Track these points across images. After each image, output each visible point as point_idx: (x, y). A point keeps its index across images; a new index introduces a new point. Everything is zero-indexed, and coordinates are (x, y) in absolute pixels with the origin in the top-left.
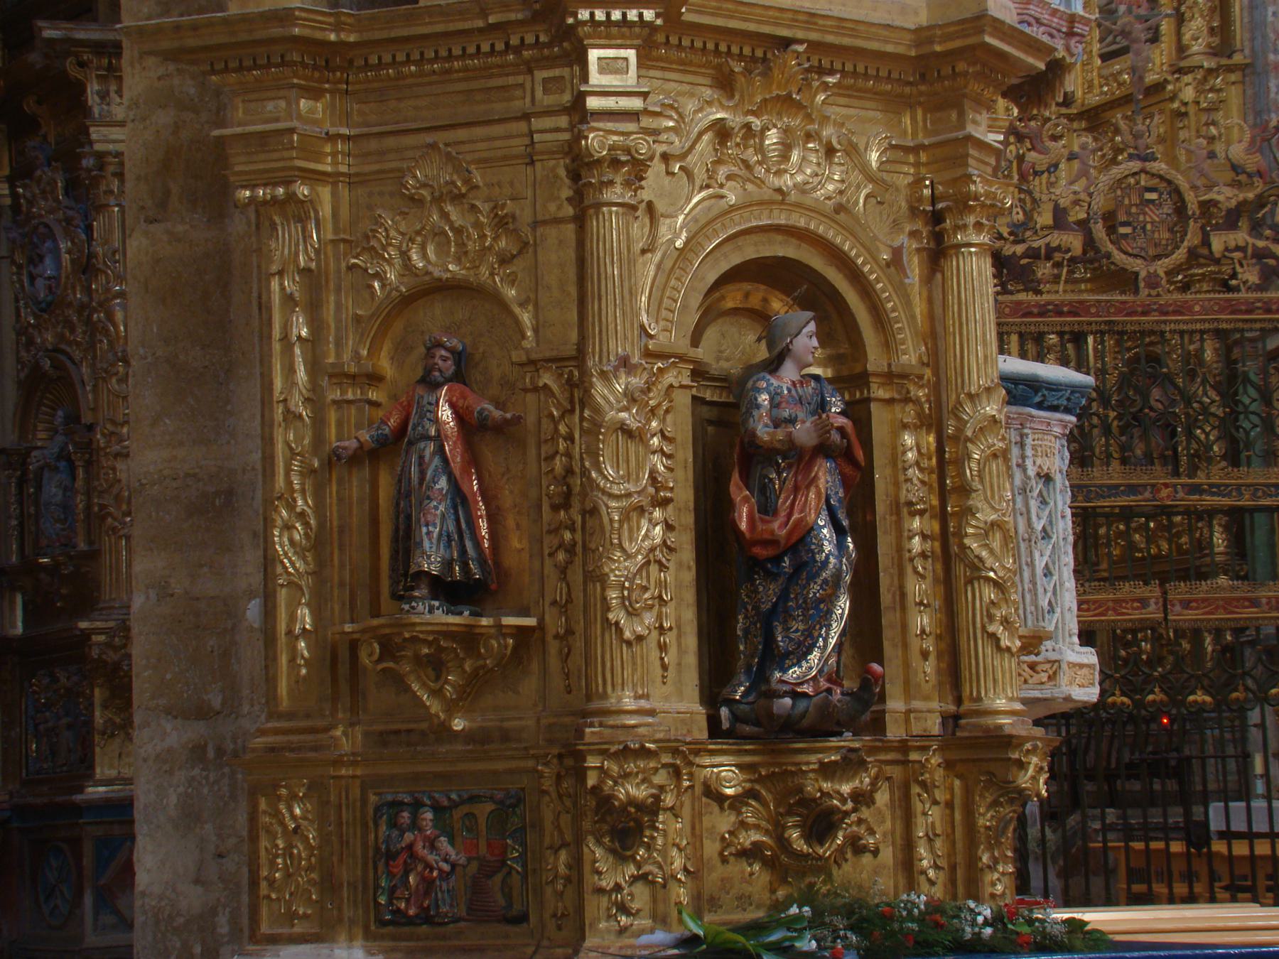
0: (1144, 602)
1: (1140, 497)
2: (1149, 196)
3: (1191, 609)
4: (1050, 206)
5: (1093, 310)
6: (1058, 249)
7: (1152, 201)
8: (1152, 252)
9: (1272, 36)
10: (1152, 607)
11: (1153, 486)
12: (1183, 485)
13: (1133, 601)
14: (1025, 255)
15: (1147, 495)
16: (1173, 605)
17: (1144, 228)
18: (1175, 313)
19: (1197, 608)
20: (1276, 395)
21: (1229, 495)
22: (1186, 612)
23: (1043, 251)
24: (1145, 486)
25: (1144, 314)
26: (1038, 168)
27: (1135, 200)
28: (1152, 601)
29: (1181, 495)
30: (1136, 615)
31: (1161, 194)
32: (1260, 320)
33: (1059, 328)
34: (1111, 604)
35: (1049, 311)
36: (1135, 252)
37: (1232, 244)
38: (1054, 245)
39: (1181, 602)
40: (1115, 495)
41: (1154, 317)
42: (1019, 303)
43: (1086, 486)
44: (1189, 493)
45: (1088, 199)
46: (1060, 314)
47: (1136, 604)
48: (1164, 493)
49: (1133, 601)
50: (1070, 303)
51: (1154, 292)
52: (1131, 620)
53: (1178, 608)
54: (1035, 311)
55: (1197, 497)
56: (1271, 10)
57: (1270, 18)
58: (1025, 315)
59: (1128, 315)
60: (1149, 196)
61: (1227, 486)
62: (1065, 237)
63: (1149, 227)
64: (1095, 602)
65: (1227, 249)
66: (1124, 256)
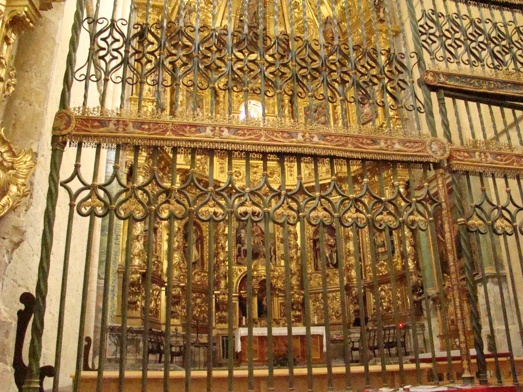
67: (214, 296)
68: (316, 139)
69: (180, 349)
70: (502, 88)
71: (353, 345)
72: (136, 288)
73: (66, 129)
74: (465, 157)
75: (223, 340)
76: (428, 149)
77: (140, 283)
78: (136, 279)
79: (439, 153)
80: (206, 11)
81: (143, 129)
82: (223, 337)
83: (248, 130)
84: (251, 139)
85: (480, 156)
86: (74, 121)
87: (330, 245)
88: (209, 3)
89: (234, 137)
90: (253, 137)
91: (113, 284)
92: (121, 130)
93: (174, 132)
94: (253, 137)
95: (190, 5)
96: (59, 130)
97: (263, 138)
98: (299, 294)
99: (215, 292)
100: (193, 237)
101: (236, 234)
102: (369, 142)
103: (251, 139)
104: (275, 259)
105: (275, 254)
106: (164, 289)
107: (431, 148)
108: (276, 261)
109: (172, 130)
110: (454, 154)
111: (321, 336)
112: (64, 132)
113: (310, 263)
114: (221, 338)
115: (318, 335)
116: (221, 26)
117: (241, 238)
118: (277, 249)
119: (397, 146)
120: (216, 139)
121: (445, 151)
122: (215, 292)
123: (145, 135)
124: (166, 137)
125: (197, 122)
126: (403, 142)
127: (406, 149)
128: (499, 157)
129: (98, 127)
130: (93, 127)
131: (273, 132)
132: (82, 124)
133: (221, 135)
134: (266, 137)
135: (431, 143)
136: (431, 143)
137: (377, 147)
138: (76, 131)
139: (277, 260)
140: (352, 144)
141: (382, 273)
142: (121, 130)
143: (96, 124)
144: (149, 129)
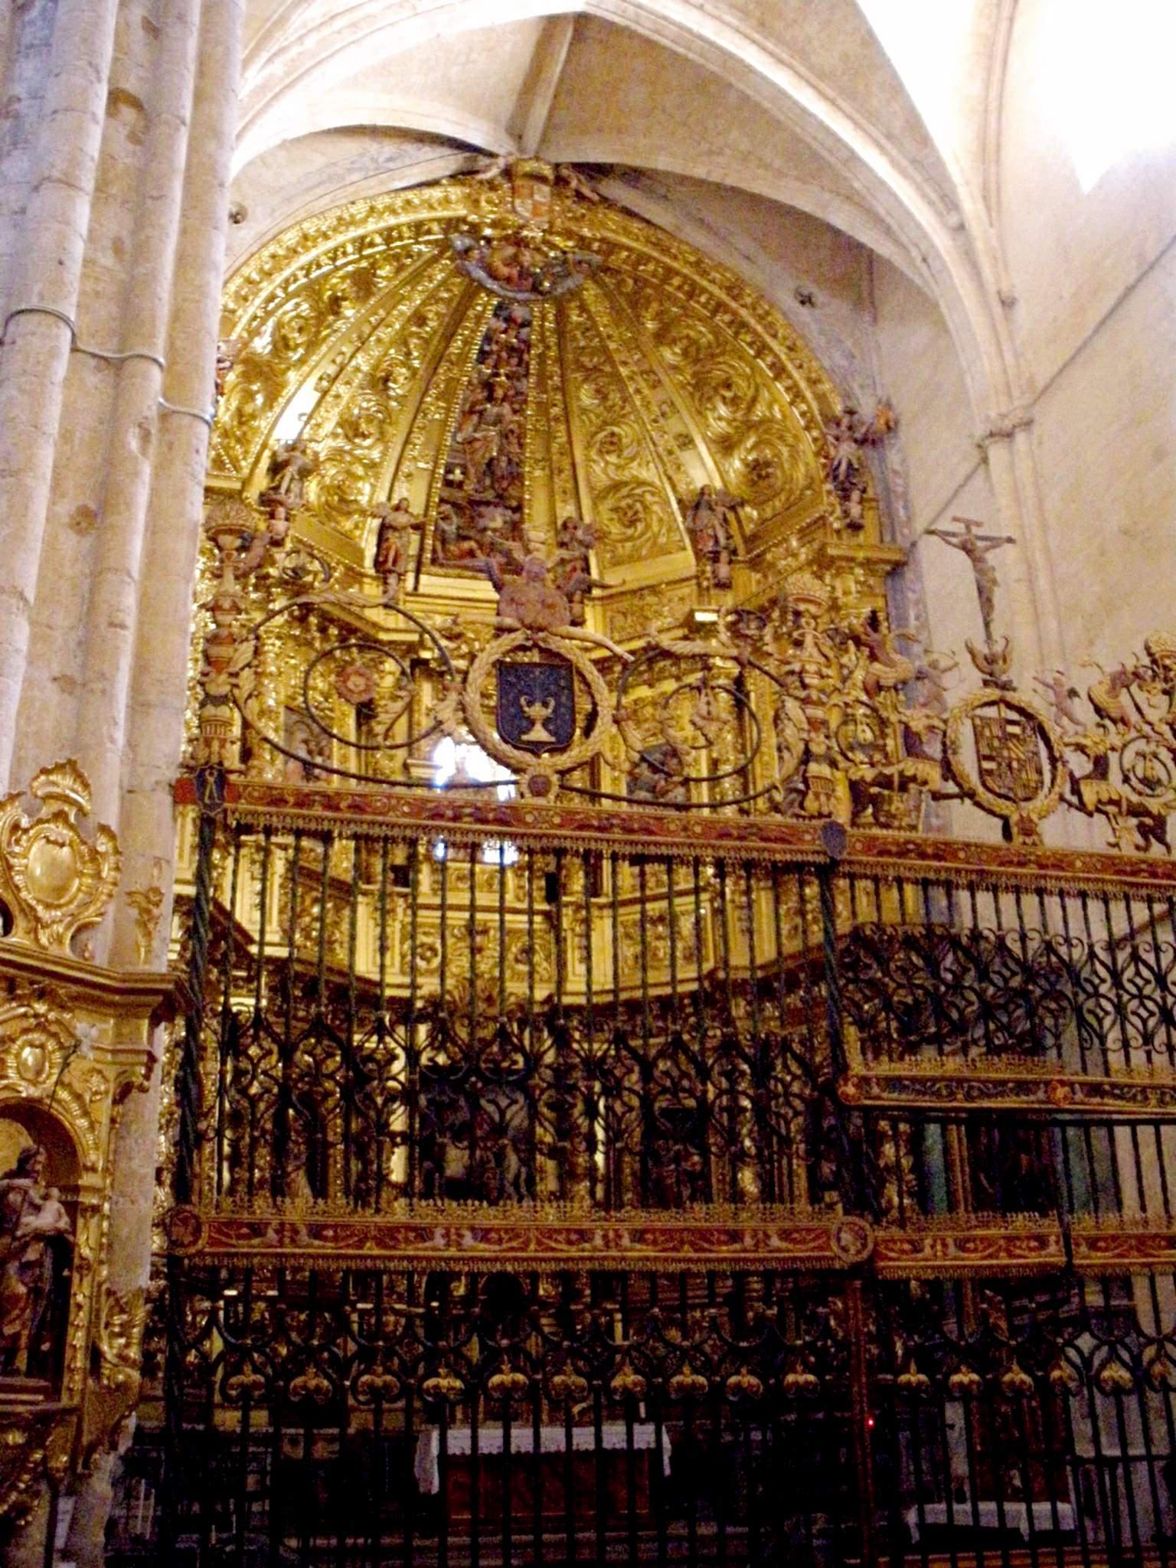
0: (1042, 1241)
1: (1032, 1098)
2: (1011, 729)
3: (1099, 1249)
4: (900, 729)
5: (962, 855)
6: (914, 779)
7: (1015, 736)
8: (1021, 793)
10: (1053, 1248)
11: (1047, 1083)
12: (1081, 1084)
13: (1028, 1238)
14: (875, 783)
15: (1041, 1095)
16: (1078, 1245)
17: (1009, 766)
18: (1055, 866)
19: (1106, 1250)
20: (1171, 978)
21: (1134, 1098)
22: (1093, 1254)
23: (896, 779)
24: (1036, 1083)
25: (1021, 864)
26: (883, 682)
27: (997, 731)
28: (1053, 1239)
29: (1079, 1096)
30: (1034, 1259)
31: (1024, 730)
32: (1146, 885)
33: (921, 875)
34: (1002, 1242)
35: (909, 851)
36: (1003, 791)
37: (1105, 797)
38: (909, 773)
39: (1087, 1239)
40: (1002, 1094)
41: (1032, 870)
42: (874, 838)
43: (968, 1080)
44: (1089, 1094)
45: (942, 725)
46: (923, 856)
47: (1033, 1244)
48: (1061, 1092)
49: (1028, 1238)
50: (935, 844)
51: (1029, 840)
52: (1026, 1266)
53: (1083, 1249)
54: (894, 849)
55: (1097, 1100)
58: (881, 853)
59: (1002, 864)
60: (1011, 729)
61: (1131, 1086)
62: (920, 766)
63: (1015, 765)
64: (983, 1239)
65: (1100, 801)
66: (990, 796)
67: (355, 1317)
68: (626, 1241)
70: (996, 1095)
73: (194, 1243)
74: (903, 1252)
76: (833, 1244)
79: (853, 1251)
80: (348, 458)
81: (325, 1239)
83: (506, 1231)
84: (512, 1249)
85: (933, 1247)
86: (205, 1228)
88: (356, 436)
89: (482, 1246)
90: (514, 1244)
92: (287, 1241)
93: (380, 1243)
94: (514, 1244)
95: (304, 452)
96: (182, 1245)
97: (532, 1246)
99: (360, 1306)
100: (297, 1146)
102: (723, 1238)
103: (512, 1249)
107: (839, 1240)
109: (374, 1238)
110: (882, 1249)
112: (192, 1250)
116: (389, 499)
119: (775, 1242)
120: (452, 1252)
121: (864, 1246)
122: (360, 1306)
123: (329, 1249)
124: (364, 1252)
125: (418, 1221)
126: (785, 1235)
127: (791, 1246)
128: (971, 1245)
129: (247, 1237)
130: (239, 1237)
131: (551, 1233)
132: (219, 1231)
133: (459, 1244)
134: (539, 1243)
135: (840, 1230)
136: (840, 1230)
137: (737, 1246)
138: (211, 1245)
140: (692, 1244)
142: (287, 1241)
143: (245, 1230)
144: (335, 1239)
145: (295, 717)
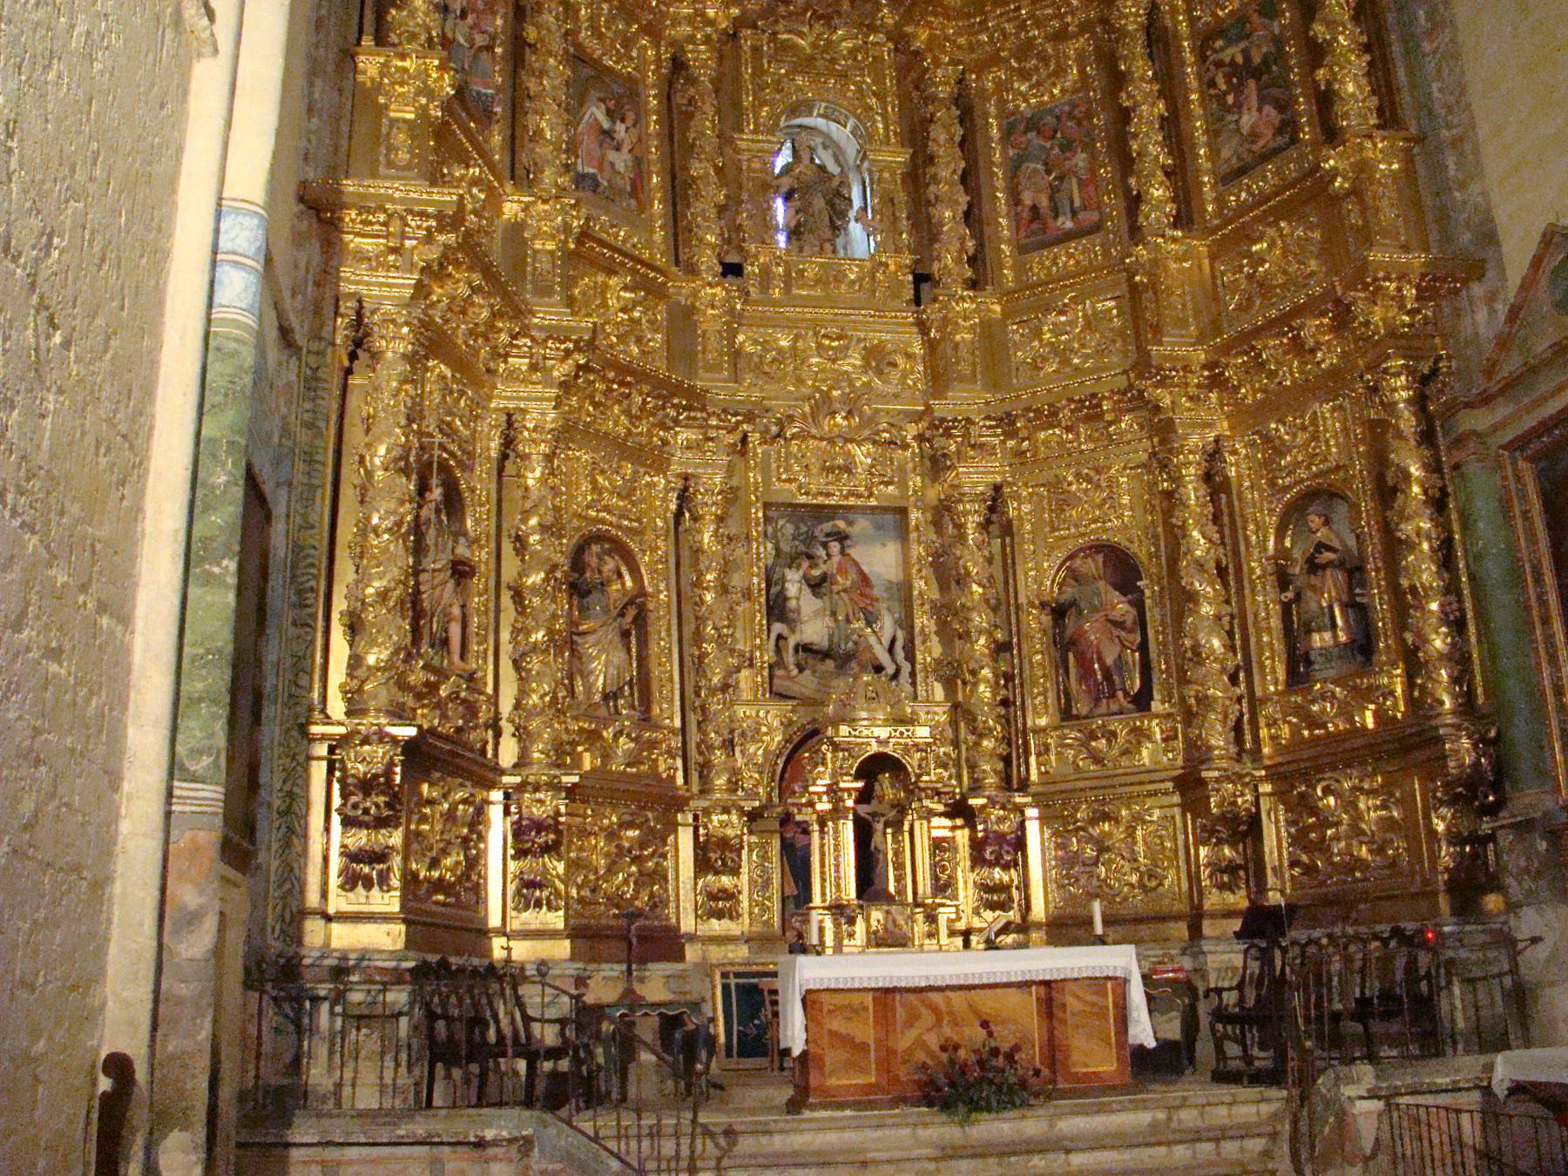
9: (1443, 112)
56: (1435, 86)
57: (1436, 94)
69: (562, 1033)
71: (1221, 999)
72: (381, 799)
75: (726, 988)
77: (398, 779)
78: (379, 768)
82: (725, 975)
87: (1119, 625)
91: (287, 787)
98: (1003, 808)
101: (768, 587)
104: (913, 674)
105: (911, 657)
106: (497, 795)
108: (914, 684)
111: (1122, 984)
113: (1044, 693)
114: (718, 976)
115: (1108, 978)
117: (786, 599)
118: (918, 641)
139: (919, 678)
141: (1324, 726)
145: (588, 71)
